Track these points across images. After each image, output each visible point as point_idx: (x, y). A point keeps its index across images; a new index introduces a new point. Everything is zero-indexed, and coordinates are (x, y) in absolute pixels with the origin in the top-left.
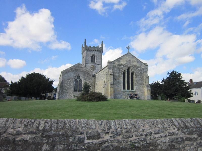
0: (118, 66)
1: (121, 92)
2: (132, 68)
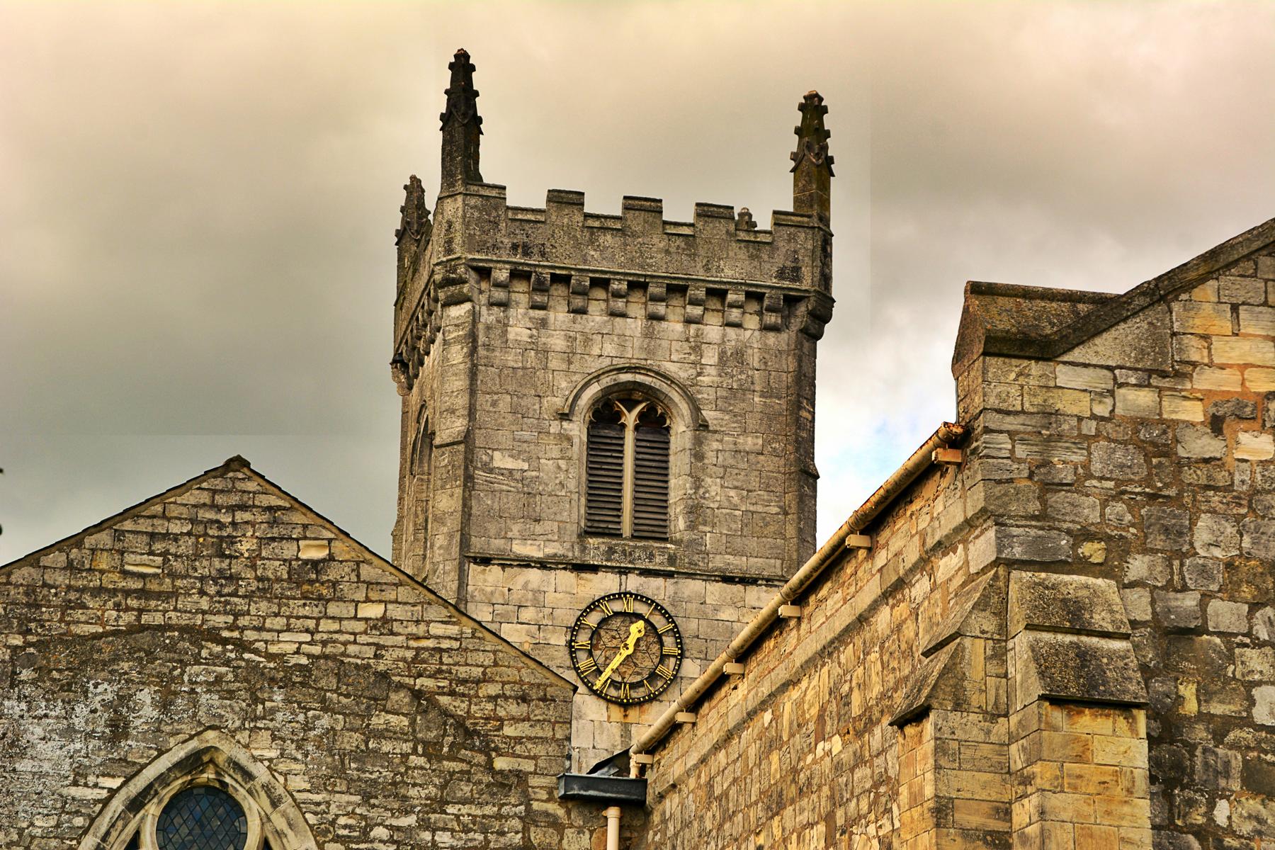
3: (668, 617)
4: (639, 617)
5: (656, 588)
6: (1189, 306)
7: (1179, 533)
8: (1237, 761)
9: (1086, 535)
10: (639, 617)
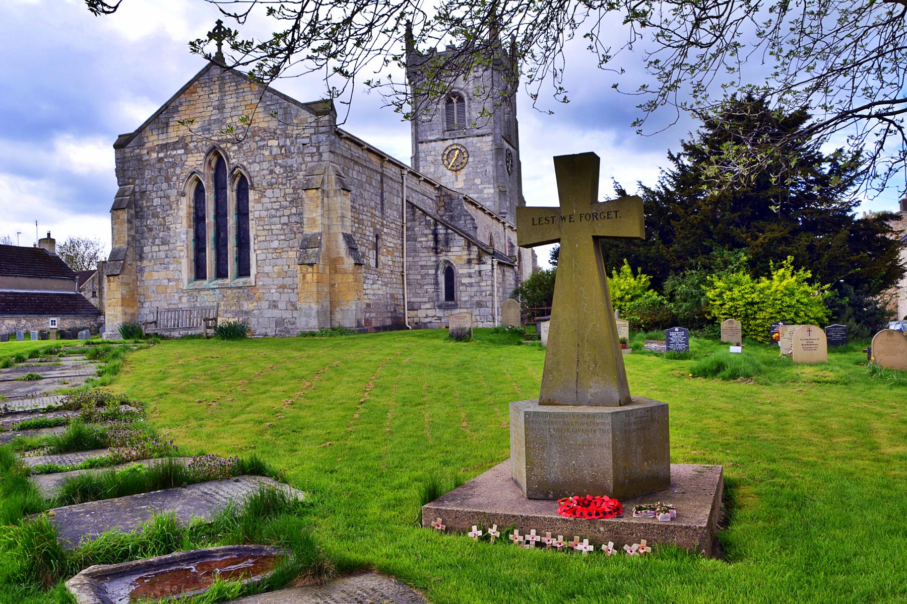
1: (177, 297)
3: (464, 148)
4: (457, 149)
5: (462, 141)
6: (145, 132)
7: (143, 174)
8: (151, 212)
9: (129, 178)
10: (457, 149)
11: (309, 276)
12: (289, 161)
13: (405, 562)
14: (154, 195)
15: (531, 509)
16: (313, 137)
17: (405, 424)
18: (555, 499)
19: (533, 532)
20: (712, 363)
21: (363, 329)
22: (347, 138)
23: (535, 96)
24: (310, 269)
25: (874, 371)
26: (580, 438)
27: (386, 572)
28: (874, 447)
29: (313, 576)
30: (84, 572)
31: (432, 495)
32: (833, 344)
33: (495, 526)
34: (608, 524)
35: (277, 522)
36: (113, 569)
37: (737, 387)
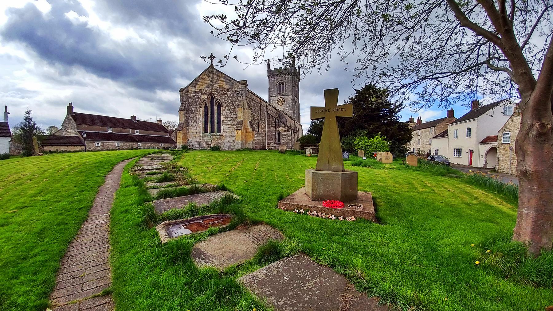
0: (193, 94)
1: (199, 138)
2: (217, 94)
5: (283, 97)
11: (239, 133)
12: (233, 99)
13: (274, 221)
14: (192, 107)
15: (313, 204)
16: (241, 91)
17: (269, 176)
18: (321, 201)
19: (315, 211)
20: (359, 162)
21: (254, 149)
22: (250, 92)
23: (319, 69)
24: (239, 131)
25: (407, 166)
26: (330, 181)
27: (268, 224)
28: (416, 189)
29: (244, 225)
30: (163, 223)
31: (281, 198)
32: (394, 159)
33: (302, 209)
34: (340, 210)
35: (232, 206)
36: (173, 222)
37: (367, 169)
